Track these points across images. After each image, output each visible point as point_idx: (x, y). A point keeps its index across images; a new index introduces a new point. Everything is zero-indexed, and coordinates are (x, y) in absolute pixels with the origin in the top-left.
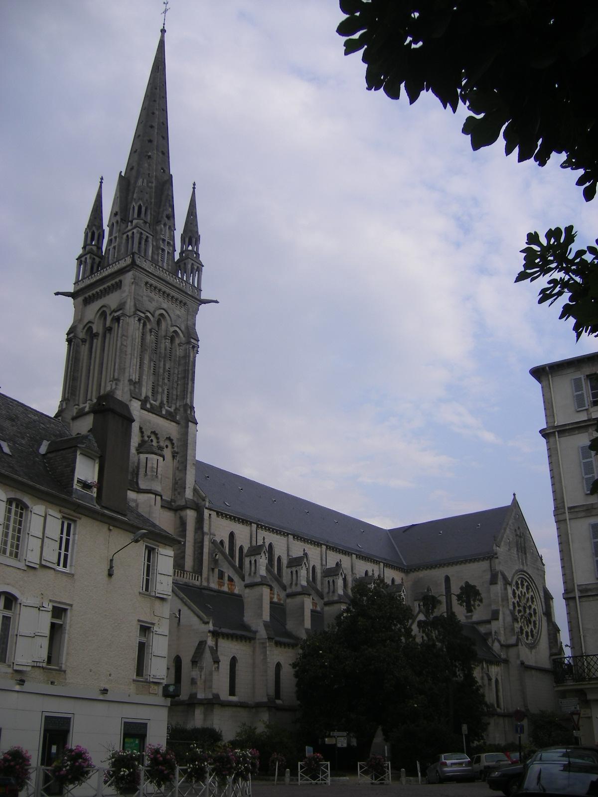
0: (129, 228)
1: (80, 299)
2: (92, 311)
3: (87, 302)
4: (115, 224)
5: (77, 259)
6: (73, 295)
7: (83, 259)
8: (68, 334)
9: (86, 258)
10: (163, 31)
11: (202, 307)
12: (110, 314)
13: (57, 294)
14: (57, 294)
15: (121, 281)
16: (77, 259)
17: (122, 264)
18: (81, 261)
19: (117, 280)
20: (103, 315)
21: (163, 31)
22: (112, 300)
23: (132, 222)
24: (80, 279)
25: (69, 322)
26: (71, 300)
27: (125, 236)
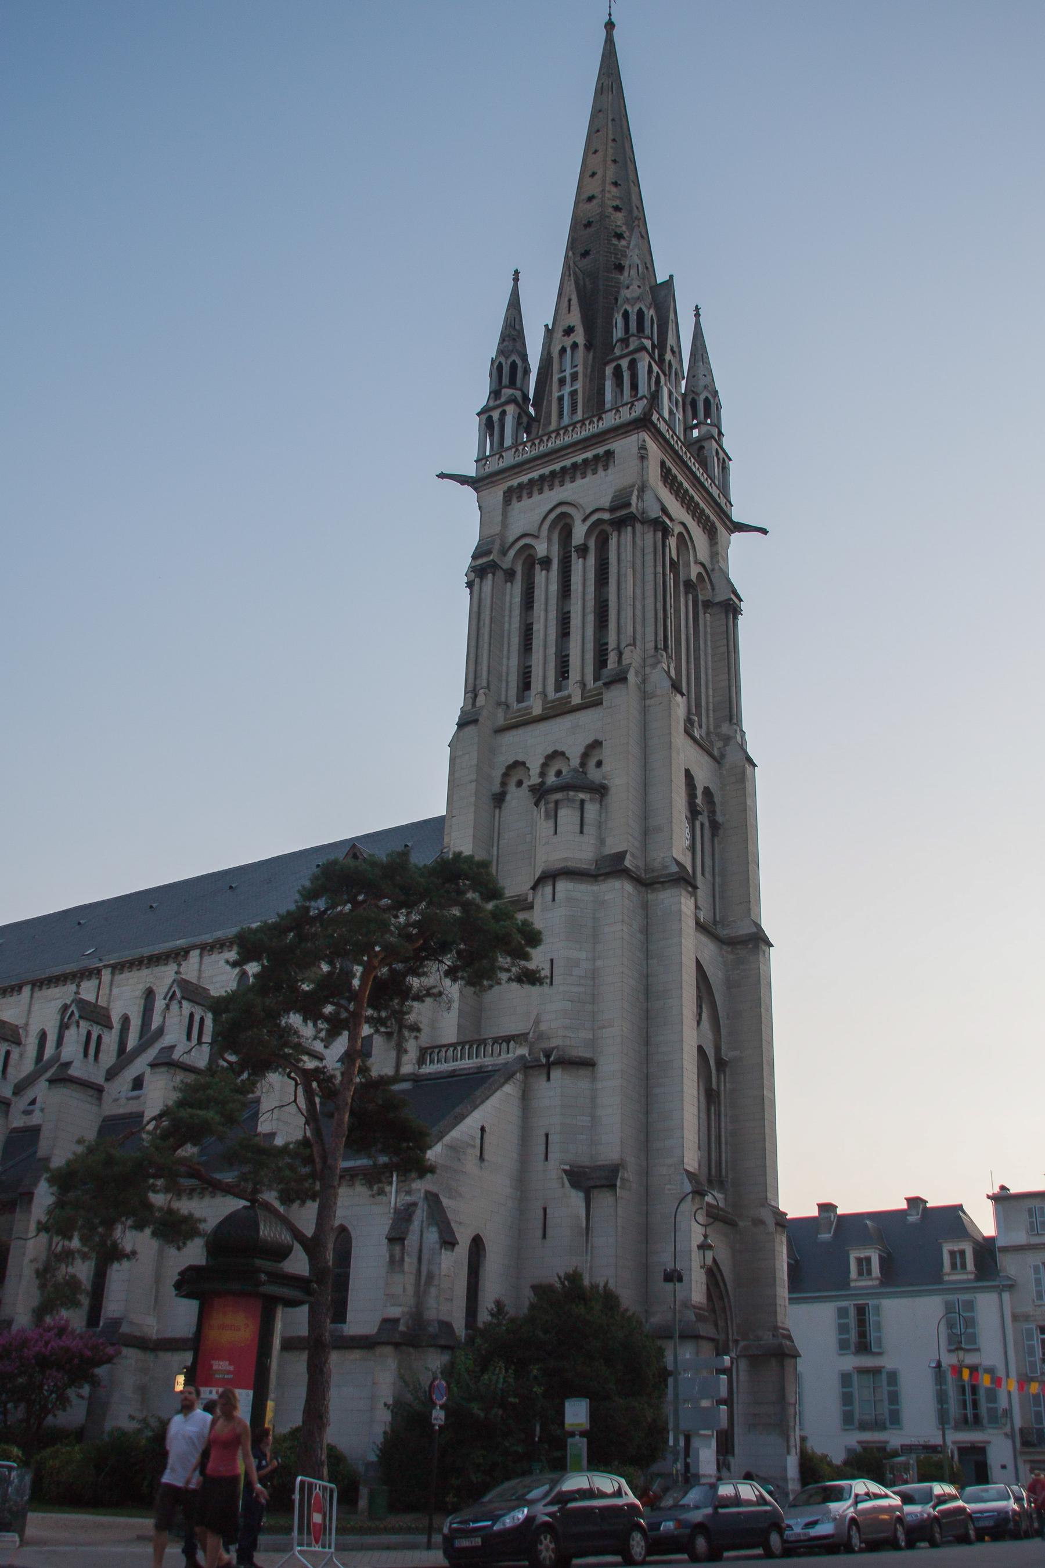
0: (617, 352)
1: (497, 494)
2: (529, 514)
3: (509, 496)
4: (569, 350)
5: (478, 414)
6: (474, 483)
7: (496, 415)
8: (474, 557)
9: (503, 413)
10: (610, 26)
11: (736, 537)
12: (584, 520)
13: (442, 476)
14: (442, 476)
15: (609, 454)
16: (478, 414)
17: (610, 420)
18: (490, 418)
19: (600, 451)
20: (562, 525)
21: (610, 26)
22: (592, 493)
23: (625, 341)
24: (488, 454)
25: (471, 540)
26: (469, 493)
27: (609, 370)
